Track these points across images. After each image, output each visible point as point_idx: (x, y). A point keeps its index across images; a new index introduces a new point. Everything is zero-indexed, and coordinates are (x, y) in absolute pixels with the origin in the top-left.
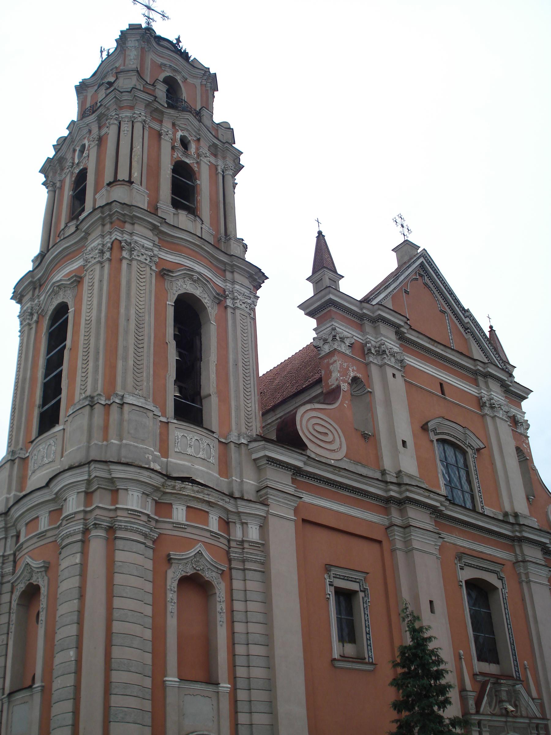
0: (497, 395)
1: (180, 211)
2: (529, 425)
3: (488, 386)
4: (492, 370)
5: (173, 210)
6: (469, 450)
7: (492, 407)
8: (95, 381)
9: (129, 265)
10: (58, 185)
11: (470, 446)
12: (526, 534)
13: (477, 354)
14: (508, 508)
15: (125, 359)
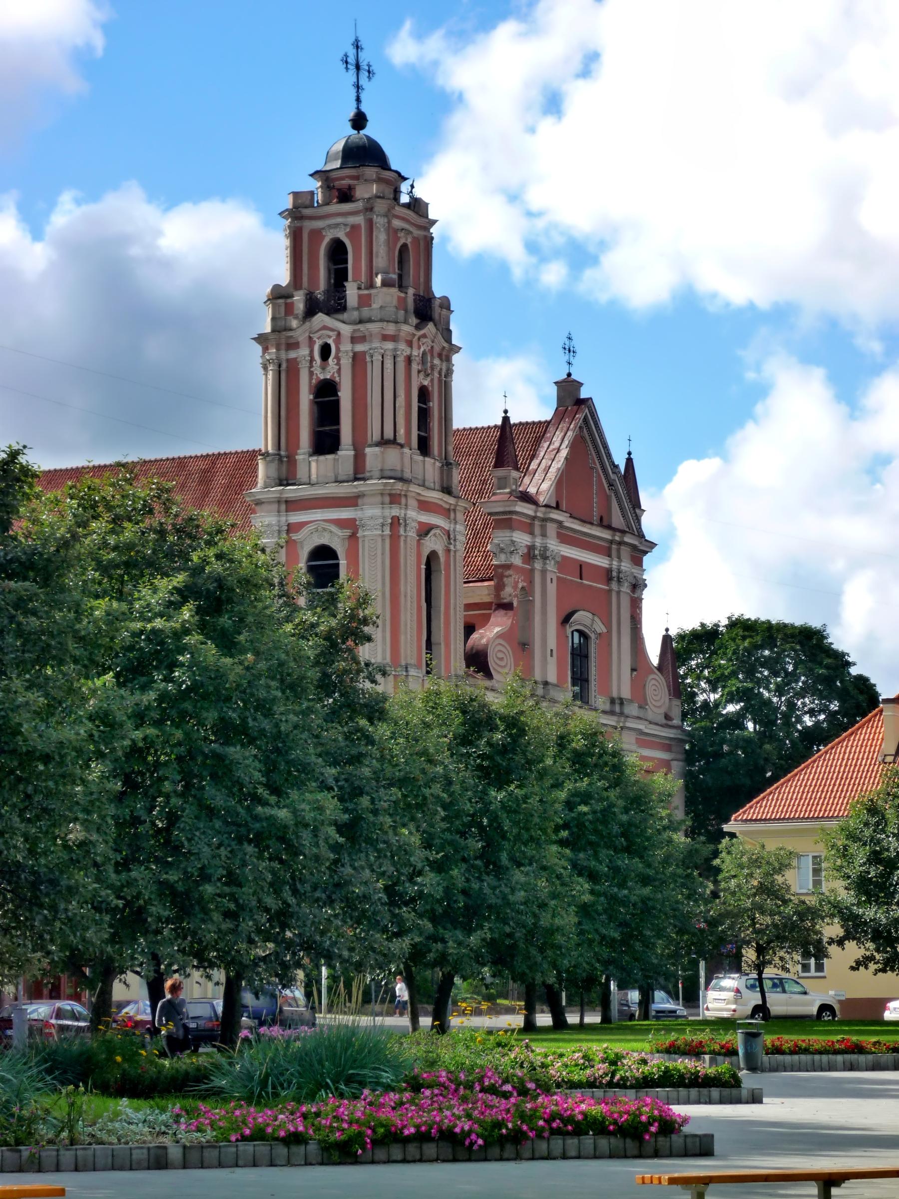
0: (626, 566)
1: (427, 459)
2: (646, 586)
3: (619, 557)
4: (628, 539)
5: (421, 458)
6: (593, 636)
7: (619, 580)
8: (384, 651)
9: (405, 541)
10: (284, 366)
11: (595, 632)
12: (628, 725)
13: (617, 520)
14: (615, 694)
15: (406, 633)
